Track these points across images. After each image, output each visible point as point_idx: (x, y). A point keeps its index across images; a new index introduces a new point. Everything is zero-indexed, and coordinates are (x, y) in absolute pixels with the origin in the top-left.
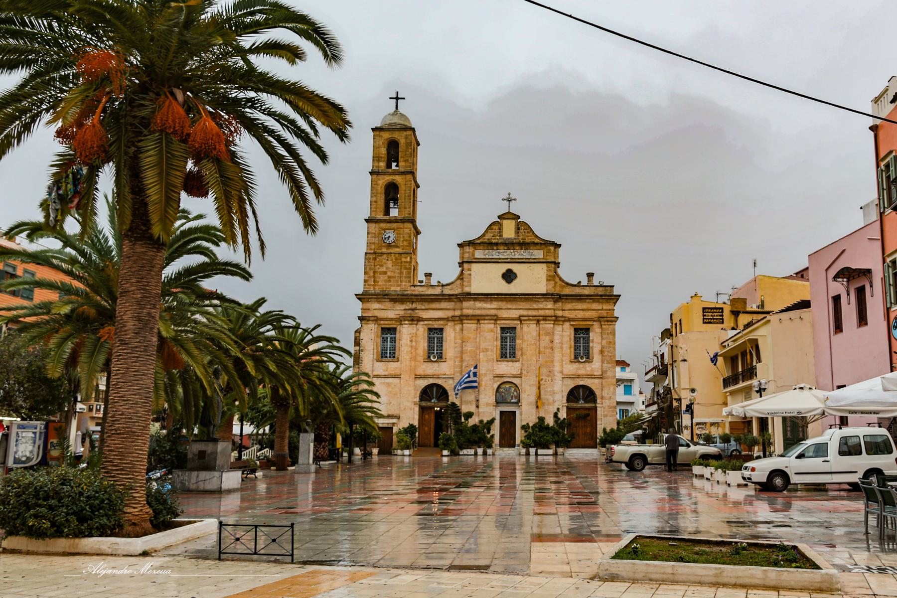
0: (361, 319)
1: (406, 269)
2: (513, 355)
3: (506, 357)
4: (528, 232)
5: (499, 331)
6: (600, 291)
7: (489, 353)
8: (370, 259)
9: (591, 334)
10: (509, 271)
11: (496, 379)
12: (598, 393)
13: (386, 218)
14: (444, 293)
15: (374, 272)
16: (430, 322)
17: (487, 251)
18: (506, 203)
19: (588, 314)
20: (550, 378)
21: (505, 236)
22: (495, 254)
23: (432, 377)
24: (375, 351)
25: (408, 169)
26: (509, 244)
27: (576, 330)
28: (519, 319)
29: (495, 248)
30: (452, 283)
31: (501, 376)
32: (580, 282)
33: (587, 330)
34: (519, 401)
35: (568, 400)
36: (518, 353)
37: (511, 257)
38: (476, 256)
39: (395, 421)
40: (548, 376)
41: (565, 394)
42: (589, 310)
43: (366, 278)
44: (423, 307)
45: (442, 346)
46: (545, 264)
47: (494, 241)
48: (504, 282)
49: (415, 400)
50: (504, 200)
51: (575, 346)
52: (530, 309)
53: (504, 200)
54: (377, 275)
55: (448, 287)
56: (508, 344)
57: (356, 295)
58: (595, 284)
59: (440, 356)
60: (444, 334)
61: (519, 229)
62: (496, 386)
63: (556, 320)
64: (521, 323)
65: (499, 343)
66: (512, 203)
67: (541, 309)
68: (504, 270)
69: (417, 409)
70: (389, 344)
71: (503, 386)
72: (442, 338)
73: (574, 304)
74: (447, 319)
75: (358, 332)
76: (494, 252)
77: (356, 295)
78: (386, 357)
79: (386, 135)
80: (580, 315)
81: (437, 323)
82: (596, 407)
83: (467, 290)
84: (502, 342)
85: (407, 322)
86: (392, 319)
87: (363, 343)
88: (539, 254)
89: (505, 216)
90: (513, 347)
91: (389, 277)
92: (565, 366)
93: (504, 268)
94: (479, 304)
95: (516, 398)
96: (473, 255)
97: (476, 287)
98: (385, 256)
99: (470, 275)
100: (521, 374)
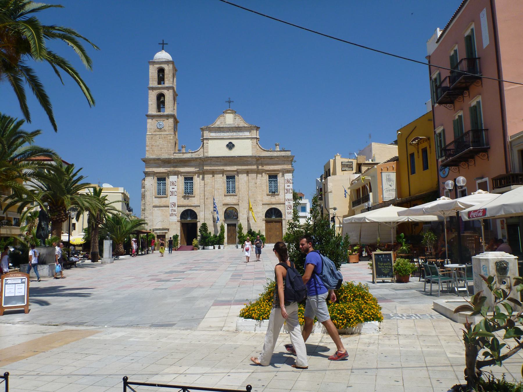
1: (170, 143)
2: (234, 191)
3: (230, 193)
5: (225, 178)
8: (149, 137)
10: (230, 143)
12: (283, 212)
13: (159, 113)
15: (152, 145)
20: (255, 204)
22: (222, 135)
23: (188, 206)
24: (154, 191)
25: (171, 85)
33: (275, 177)
34: (238, 218)
35: (266, 216)
36: (237, 190)
40: (254, 203)
45: (192, 187)
47: (221, 126)
48: (227, 150)
50: (226, 102)
51: (269, 185)
53: (226, 102)
56: (231, 185)
57: (142, 159)
59: (192, 193)
60: (194, 180)
61: (235, 118)
62: (224, 210)
63: (258, 172)
65: (226, 185)
70: (162, 187)
74: (195, 173)
77: (142, 159)
78: (160, 194)
83: (206, 155)
84: (227, 184)
87: (146, 187)
90: (234, 187)
91: (161, 148)
93: (227, 142)
95: (236, 216)
99: (208, 146)
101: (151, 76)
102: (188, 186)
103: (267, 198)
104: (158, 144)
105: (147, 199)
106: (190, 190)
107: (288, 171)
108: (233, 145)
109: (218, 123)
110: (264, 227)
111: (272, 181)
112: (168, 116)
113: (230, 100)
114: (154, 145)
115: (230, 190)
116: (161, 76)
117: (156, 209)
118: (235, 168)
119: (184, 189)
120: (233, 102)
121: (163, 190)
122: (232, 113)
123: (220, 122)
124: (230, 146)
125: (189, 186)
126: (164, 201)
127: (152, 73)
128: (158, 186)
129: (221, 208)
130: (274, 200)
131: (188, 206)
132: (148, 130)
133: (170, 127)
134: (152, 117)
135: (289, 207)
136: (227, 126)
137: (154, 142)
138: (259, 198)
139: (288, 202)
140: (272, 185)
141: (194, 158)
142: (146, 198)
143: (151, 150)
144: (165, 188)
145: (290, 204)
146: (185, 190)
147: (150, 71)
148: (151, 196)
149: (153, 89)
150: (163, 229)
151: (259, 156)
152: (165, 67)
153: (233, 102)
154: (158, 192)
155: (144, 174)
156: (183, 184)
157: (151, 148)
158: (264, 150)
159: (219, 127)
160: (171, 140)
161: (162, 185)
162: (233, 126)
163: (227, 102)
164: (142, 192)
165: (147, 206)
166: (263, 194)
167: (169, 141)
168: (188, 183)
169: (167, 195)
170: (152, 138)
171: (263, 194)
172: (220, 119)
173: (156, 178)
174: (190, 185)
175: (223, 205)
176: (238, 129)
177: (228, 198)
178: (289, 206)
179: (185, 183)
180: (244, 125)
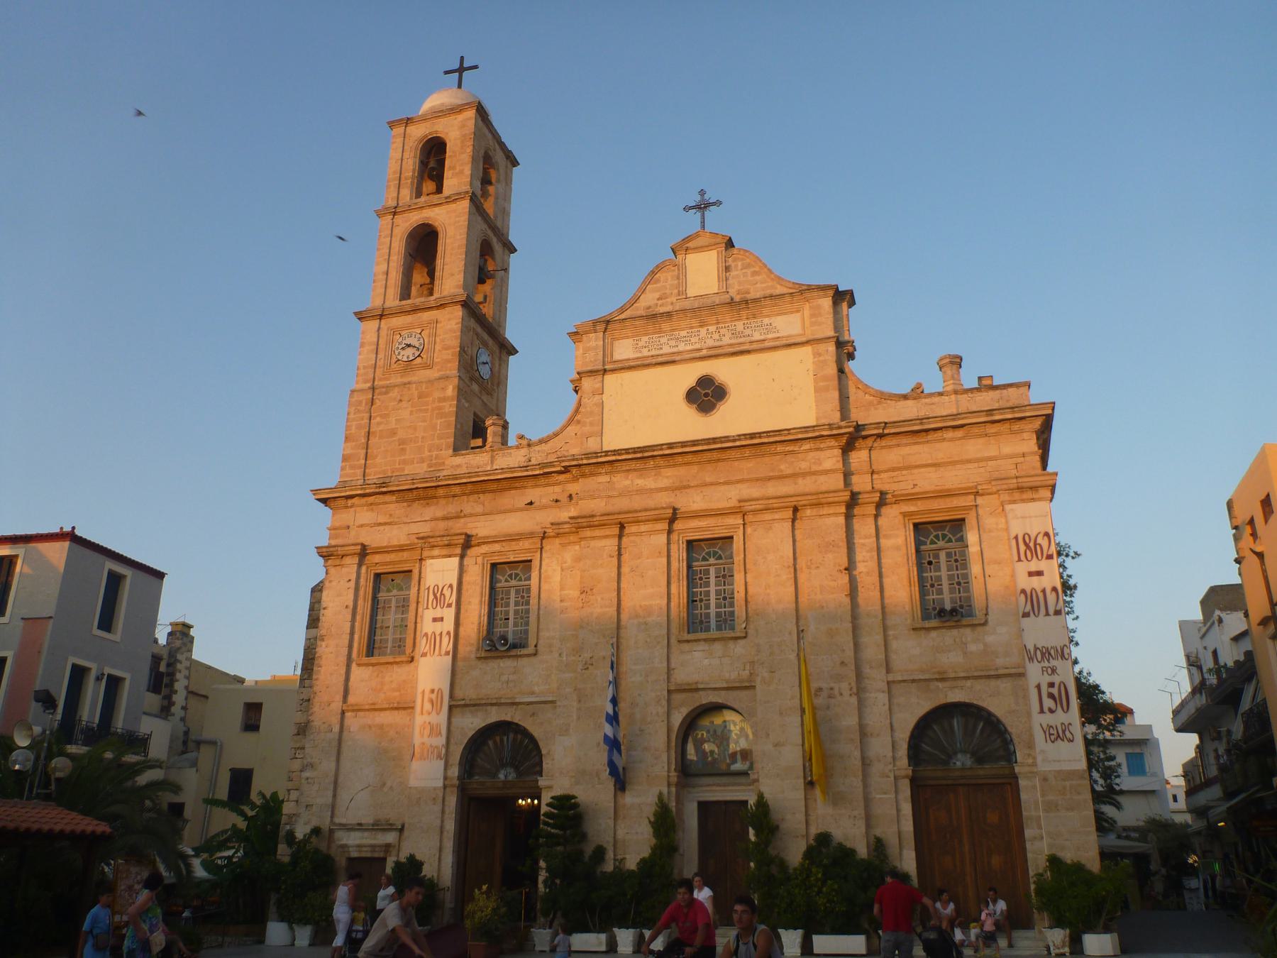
0: (326, 554)
3: (708, 629)
4: (755, 273)
5: (679, 552)
6: (986, 400)
8: (361, 402)
9: (972, 537)
11: (677, 697)
12: (1013, 726)
16: (497, 547)
17: (645, 339)
18: (695, 216)
19: (954, 478)
20: (845, 686)
21: (691, 292)
26: (703, 311)
27: (919, 528)
28: (740, 511)
29: (666, 326)
30: (556, 435)
31: (693, 689)
32: (919, 386)
33: (957, 525)
37: (710, 343)
38: (617, 357)
39: (390, 838)
41: (903, 735)
42: (954, 463)
43: (349, 451)
44: (479, 509)
46: (808, 350)
47: (662, 310)
48: (690, 412)
50: (687, 209)
52: (770, 479)
53: (687, 209)
54: (373, 441)
55: (544, 447)
56: (712, 589)
58: (966, 386)
61: (727, 269)
62: (677, 719)
66: (711, 213)
67: (804, 475)
68: (691, 381)
69: (452, 801)
73: (906, 450)
75: (317, 590)
76: (664, 340)
77: (315, 492)
79: (419, 132)
80: (927, 481)
81: (514, 546)
82: (1015, 777)
85: (436, 552)
86: (401, 549)
87: (327, 617)
88: (787, 324)
89: (690, 245)
91: (402, 442)
92: (894, 645)
93: (688, 375)
94: (622, 481)
97: (617, 437)
98: (395, 393)
104: (393, 425)
110: (908, 826)
113: (706, 197)
116: (432, 164)
120: (718, 203)
123: (657, 295)
124: (706, 395)
133: (447, 349)
135: (1051, 696)
137: (378, 419)
139: (1043, 670)
140: (939, 579)
145: (1056, 679)
150: (380, 826)
153: (718, 203)
155: (321, 560)
160: (446, 404)
167: (439, 408)
172: (658, 281)
178: (1055, 691)
180: (768, 292)
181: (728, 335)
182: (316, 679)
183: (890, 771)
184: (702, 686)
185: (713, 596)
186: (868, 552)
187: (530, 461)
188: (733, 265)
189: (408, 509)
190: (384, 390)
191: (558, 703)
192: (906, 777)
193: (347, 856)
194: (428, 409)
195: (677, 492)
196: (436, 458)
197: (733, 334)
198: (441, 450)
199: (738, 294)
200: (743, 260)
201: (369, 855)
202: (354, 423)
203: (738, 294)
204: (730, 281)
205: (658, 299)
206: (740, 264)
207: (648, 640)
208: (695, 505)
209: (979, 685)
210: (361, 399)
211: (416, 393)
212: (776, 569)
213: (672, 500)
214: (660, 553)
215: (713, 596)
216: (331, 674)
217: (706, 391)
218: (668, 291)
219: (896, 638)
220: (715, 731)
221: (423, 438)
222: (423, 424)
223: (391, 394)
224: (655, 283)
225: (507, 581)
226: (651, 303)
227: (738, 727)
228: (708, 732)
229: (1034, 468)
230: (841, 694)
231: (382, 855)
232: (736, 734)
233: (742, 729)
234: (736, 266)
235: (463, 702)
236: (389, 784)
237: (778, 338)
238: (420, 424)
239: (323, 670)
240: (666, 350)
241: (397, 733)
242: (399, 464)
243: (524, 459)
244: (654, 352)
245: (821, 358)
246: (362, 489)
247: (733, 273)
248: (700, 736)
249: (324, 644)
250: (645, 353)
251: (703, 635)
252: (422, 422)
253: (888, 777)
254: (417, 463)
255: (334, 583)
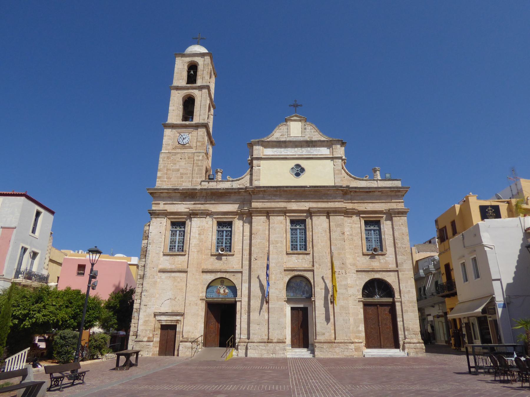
1: (198, 166)
3: (297, 249)
4: (314, 132)
7: (279, 245)
8: (165, 157)
10: (298, 166)
12: (395, 286)
14: (234, 187)
15: (167, 170)
20: (343, 271)
23: (221, 272)
33: (377, 223)
35: (364, 295)
36: (309, 245)
39: (178, 318)
40: (342, 268)
45: (231, 239)
47: (282, 140)
49: (201, 295)
56: (298, 236)
62: (287, 279)
63: (347, 213)
64: (311, 217)
69: (202, 306)
70: (178, 237)
71: (293, 281)
72: (231, 231)
80: (370, 207)
83: (256, 183)
84: (292, 234)
91: (181, 174)
95: (307, 293)
96: (263, 153)
98: (179, 156)
99: (259, 170)
100: (313, 266)
101: (177, 73)
102: (222, 236)
103: (365, 261)
104: (178, 167)
105: (150, 258)
106: (226, 243)
107: (401, 213)
108: (303, 170)
109: (277, 135)
111: (371, 230)
112: (197, 126)
114: (170, 169)
115: (297, 245)
117: (164, 275)
118: (305, 206)
119: (215, 241)
120: (301, 105)
121: (179, 243)
122: (300, 121)
123: (280, 134)
125: (224, 237)
126: (179, 263)
127: (178, 69)
128: (171, 236)
129: (281, 276)
130: (376, 264)
131: (221, 272)
132: (164, 146)
133: (199, 142)
134: (173, 126)
136: (291, 139)
137: (172, 164)
138: (349, 260)
141: (235, 189)
142: (148, 256)
143: (166, 176)
144: (184, 239)
146: (218, 243)
147: (176, 66)
148: (157, 252)
149: (178, 88)
151: (348, 187)
152: (199, 60)
153: (301, 105)
154: (171, 246)
156: (215, 232)
157: (167, 174)
158: (355, 179)
159: (279, 140)
160: (199, 162)
161: (178, 235)
162: (302, 139)
163: (292, 106)
164: (143, 245)
165: (147, 269)
166: (356, 253)
167: (197, 163)
168: (223, 231)
169: (186, 251)
170: (168, 158)
171: (356, 253)
172: (281, 129)
173: (169, 222)
174: (226, 236)
175: (285, 270)
176: (311, 144)
177: (294, 257)
179: (218, 231)
181: (305, 151)
182: (148, 259)
183: (357, 299)
184: (296, 269)
185: (298, 239)
186: (350, 228)
187: (232, 186)
188: (307, 128)
189: (185, 199)
190: (174, 154)
191: (243, 272)
192: (362, 301)
193: (161, 323)
194: (192, 163)
195: (287, 203)
196: (195, 181)
197: (307, 151)
198: (198, 179)
199: (309, 138)
200: (310, 126)
201: (170, 324)
202: (162, 165)
203: (309, 138)
204: (306, 133)
205: (281, 136)
206: (309, 128)
207: (277, 252)
208: (294, 207)
209: (384, 273)
210: (164, 156)
211: (187, 156)
212: (321, 231)
213: (286, 205)
214: (281, 223)
215: (298, 239)
216: (154, 257)
217: (298, 169)
218: (284, 134)
219: (358, 256)
220: (297, 284)
221: (190, 173)
222: (190, 168)
223: (177, 156)
224: (280, 130)
225: (222, 228)
226: (278, 137)
227: (305, 283)
228: (295, 284)
229: (402, 206)
230: (342, 274)
231: (175, 324)
232: (304, 285)
233: (306, 284)
234: (308, 128)
235: (207, 270)
236: (177, 299)
237: (322, 155)
238: (189, 168)
239: (150, 256)
240: (283, 153)
241: (181, 280)
242: (181, 182)
243: (230, 185)
244: (279, 154)
245: (337, 163)
246: (167, 190)
247: (308, 131)
248: (292, 285)
249: (151, 246)
250: (276, 154)
251: (295, 252)
252: (189, 167)
253: (356, 301)
254: (188, 182)
255: (154, 223)
